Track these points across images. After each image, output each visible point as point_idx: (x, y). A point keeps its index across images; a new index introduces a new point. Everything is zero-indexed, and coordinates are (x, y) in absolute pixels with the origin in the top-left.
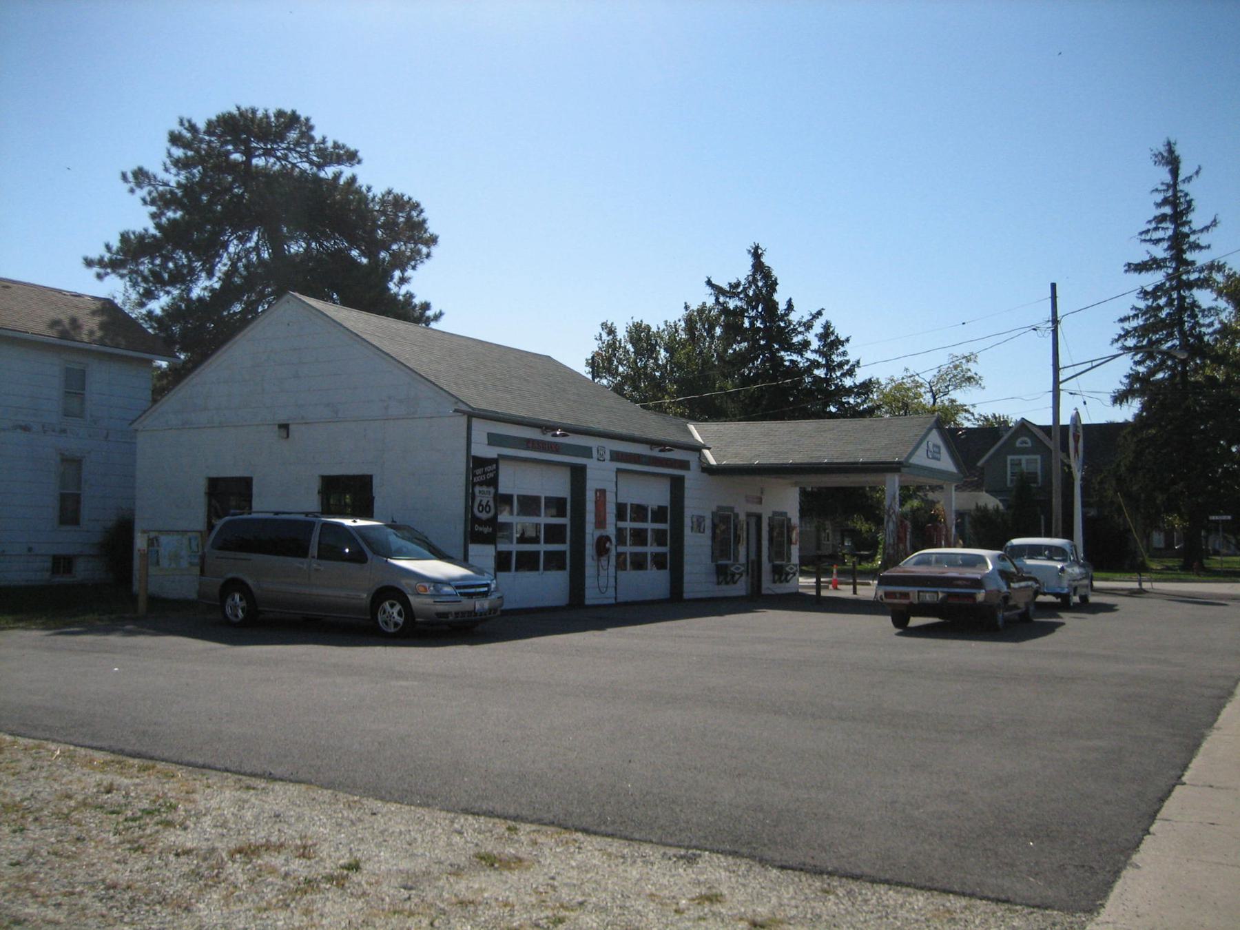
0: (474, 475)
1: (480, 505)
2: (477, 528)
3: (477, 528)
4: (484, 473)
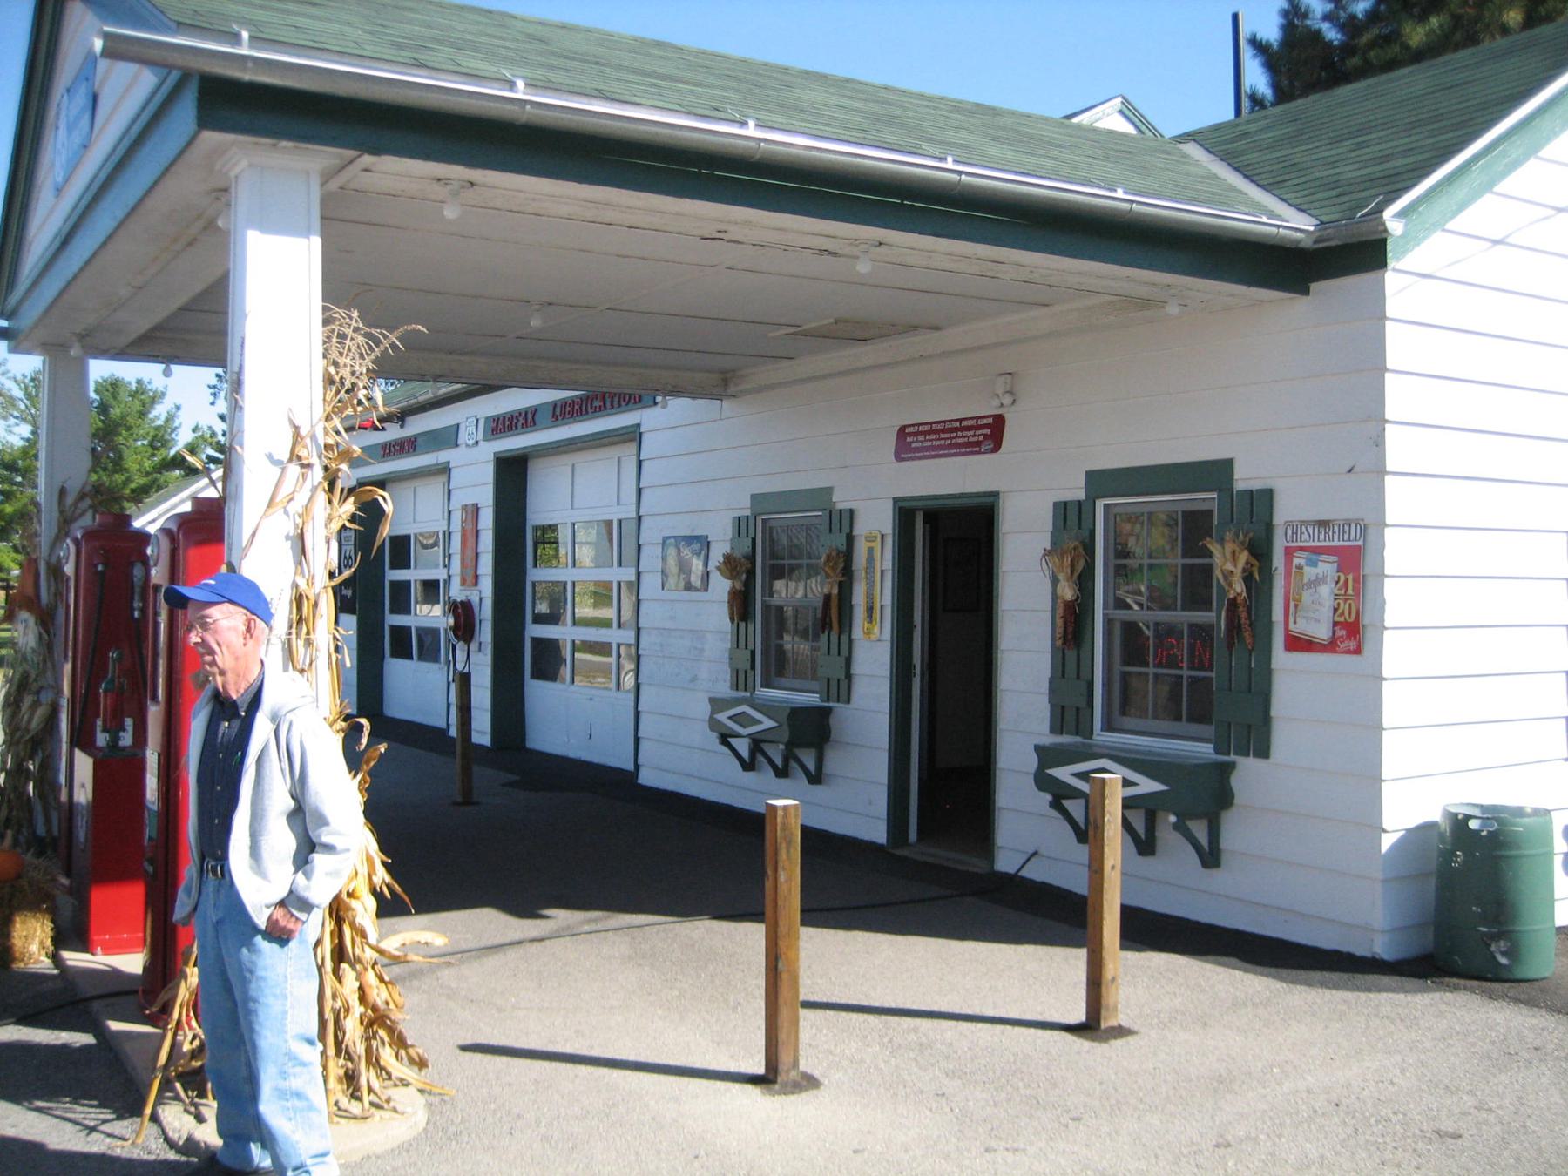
1: (345, 557)
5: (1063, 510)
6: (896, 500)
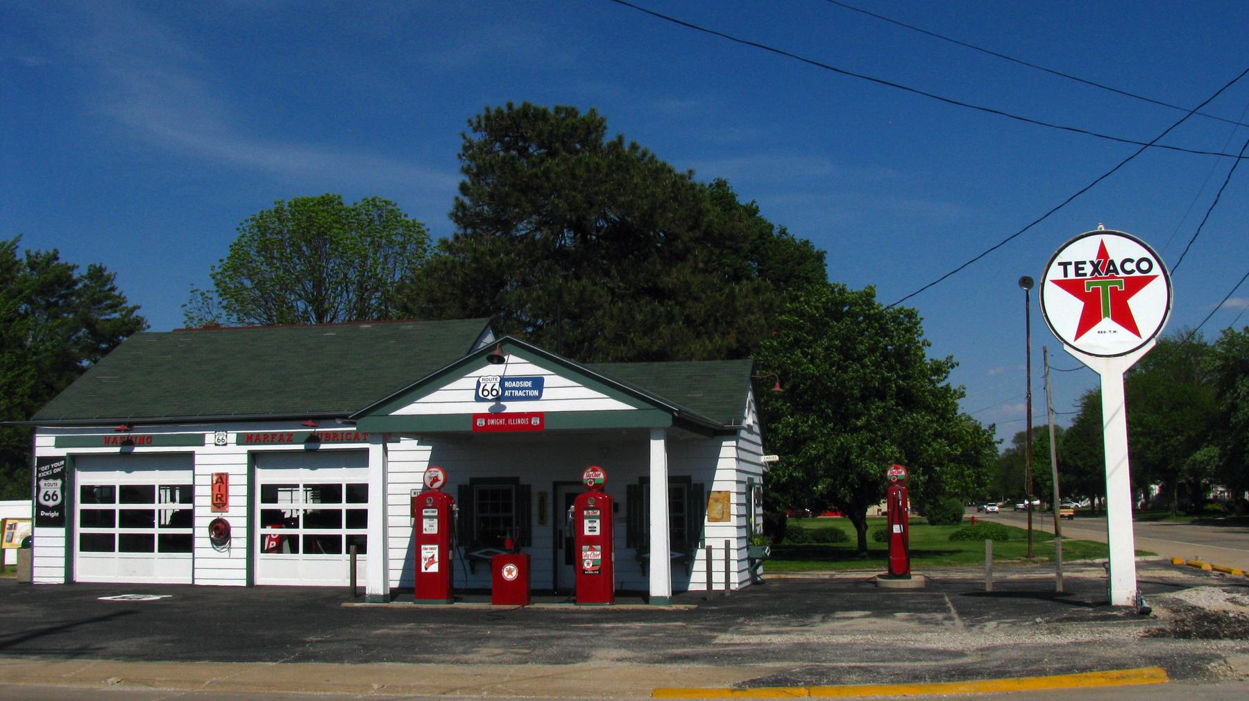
1: (46, 494)
2: (43, 513)
3: (43, 513)
4: (50, 468)
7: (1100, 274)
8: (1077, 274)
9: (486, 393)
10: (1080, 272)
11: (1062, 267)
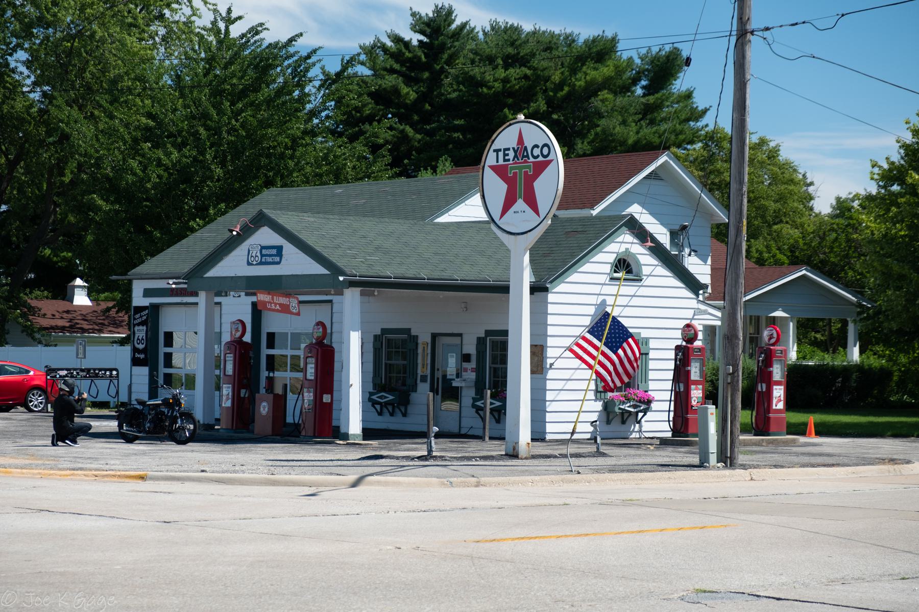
0: (135, 319)
1: (138, 339)
2: (137, 355)
3: (137, 355)
4: (141, 317)
5: (479, 339)
6: (432, 334)
7: (518, 160)
8: (505, 160)
9: (252, 259)
10: (507, 158)
11: (496, 153)
